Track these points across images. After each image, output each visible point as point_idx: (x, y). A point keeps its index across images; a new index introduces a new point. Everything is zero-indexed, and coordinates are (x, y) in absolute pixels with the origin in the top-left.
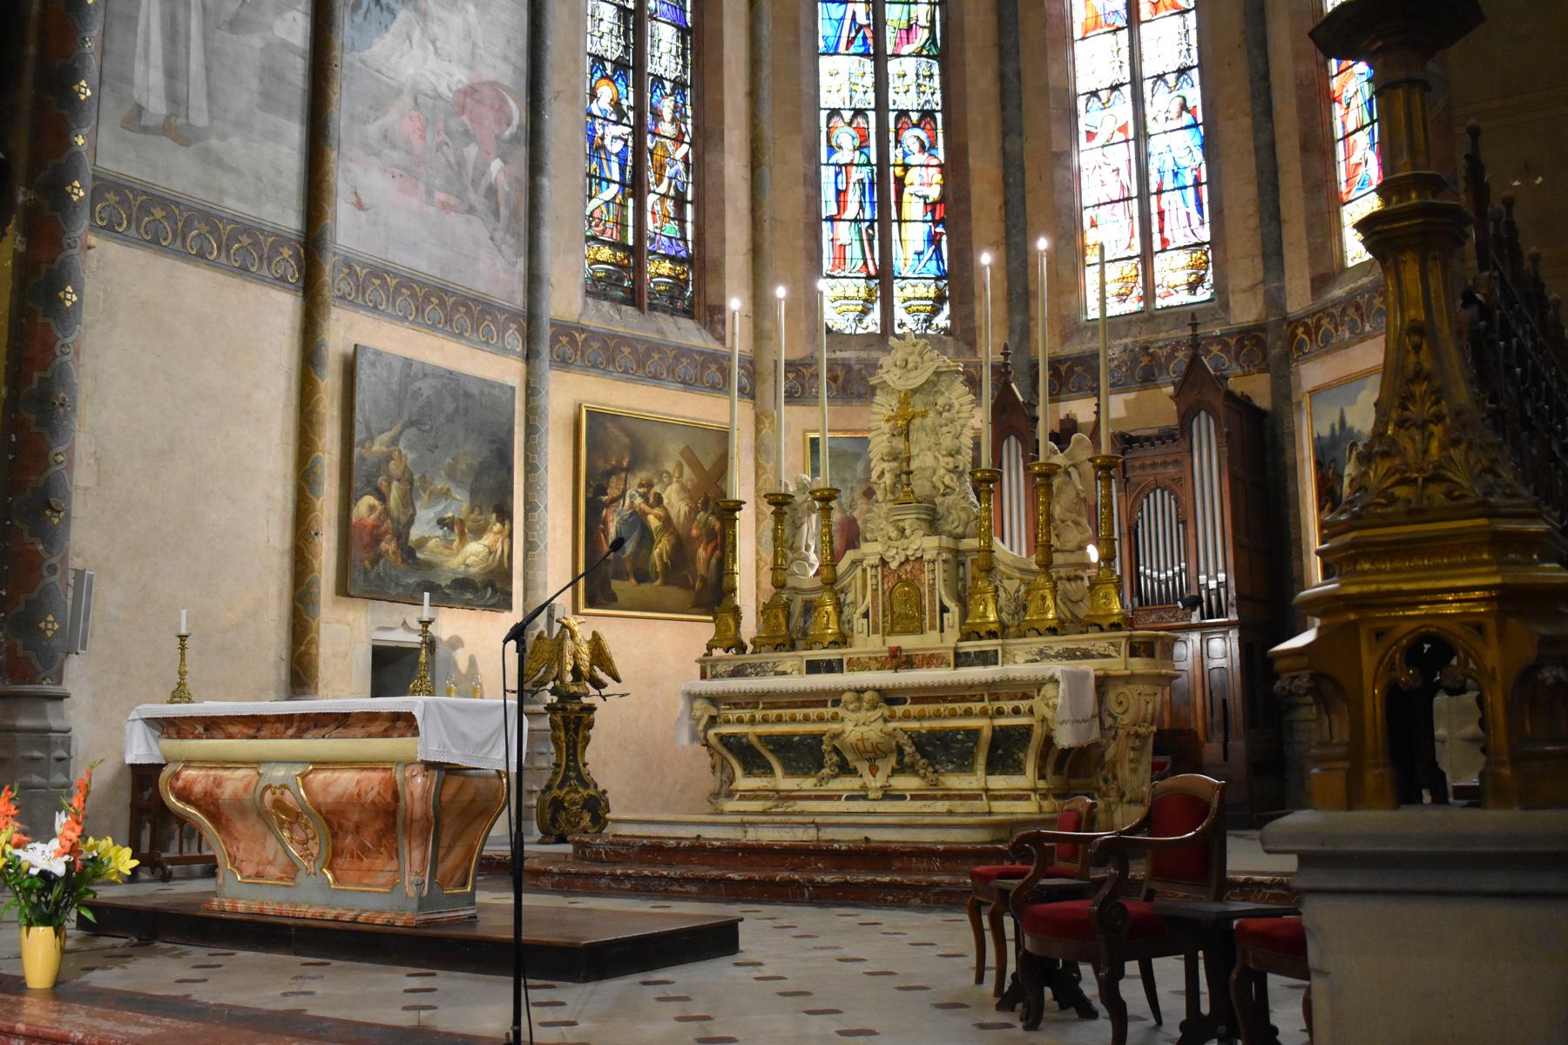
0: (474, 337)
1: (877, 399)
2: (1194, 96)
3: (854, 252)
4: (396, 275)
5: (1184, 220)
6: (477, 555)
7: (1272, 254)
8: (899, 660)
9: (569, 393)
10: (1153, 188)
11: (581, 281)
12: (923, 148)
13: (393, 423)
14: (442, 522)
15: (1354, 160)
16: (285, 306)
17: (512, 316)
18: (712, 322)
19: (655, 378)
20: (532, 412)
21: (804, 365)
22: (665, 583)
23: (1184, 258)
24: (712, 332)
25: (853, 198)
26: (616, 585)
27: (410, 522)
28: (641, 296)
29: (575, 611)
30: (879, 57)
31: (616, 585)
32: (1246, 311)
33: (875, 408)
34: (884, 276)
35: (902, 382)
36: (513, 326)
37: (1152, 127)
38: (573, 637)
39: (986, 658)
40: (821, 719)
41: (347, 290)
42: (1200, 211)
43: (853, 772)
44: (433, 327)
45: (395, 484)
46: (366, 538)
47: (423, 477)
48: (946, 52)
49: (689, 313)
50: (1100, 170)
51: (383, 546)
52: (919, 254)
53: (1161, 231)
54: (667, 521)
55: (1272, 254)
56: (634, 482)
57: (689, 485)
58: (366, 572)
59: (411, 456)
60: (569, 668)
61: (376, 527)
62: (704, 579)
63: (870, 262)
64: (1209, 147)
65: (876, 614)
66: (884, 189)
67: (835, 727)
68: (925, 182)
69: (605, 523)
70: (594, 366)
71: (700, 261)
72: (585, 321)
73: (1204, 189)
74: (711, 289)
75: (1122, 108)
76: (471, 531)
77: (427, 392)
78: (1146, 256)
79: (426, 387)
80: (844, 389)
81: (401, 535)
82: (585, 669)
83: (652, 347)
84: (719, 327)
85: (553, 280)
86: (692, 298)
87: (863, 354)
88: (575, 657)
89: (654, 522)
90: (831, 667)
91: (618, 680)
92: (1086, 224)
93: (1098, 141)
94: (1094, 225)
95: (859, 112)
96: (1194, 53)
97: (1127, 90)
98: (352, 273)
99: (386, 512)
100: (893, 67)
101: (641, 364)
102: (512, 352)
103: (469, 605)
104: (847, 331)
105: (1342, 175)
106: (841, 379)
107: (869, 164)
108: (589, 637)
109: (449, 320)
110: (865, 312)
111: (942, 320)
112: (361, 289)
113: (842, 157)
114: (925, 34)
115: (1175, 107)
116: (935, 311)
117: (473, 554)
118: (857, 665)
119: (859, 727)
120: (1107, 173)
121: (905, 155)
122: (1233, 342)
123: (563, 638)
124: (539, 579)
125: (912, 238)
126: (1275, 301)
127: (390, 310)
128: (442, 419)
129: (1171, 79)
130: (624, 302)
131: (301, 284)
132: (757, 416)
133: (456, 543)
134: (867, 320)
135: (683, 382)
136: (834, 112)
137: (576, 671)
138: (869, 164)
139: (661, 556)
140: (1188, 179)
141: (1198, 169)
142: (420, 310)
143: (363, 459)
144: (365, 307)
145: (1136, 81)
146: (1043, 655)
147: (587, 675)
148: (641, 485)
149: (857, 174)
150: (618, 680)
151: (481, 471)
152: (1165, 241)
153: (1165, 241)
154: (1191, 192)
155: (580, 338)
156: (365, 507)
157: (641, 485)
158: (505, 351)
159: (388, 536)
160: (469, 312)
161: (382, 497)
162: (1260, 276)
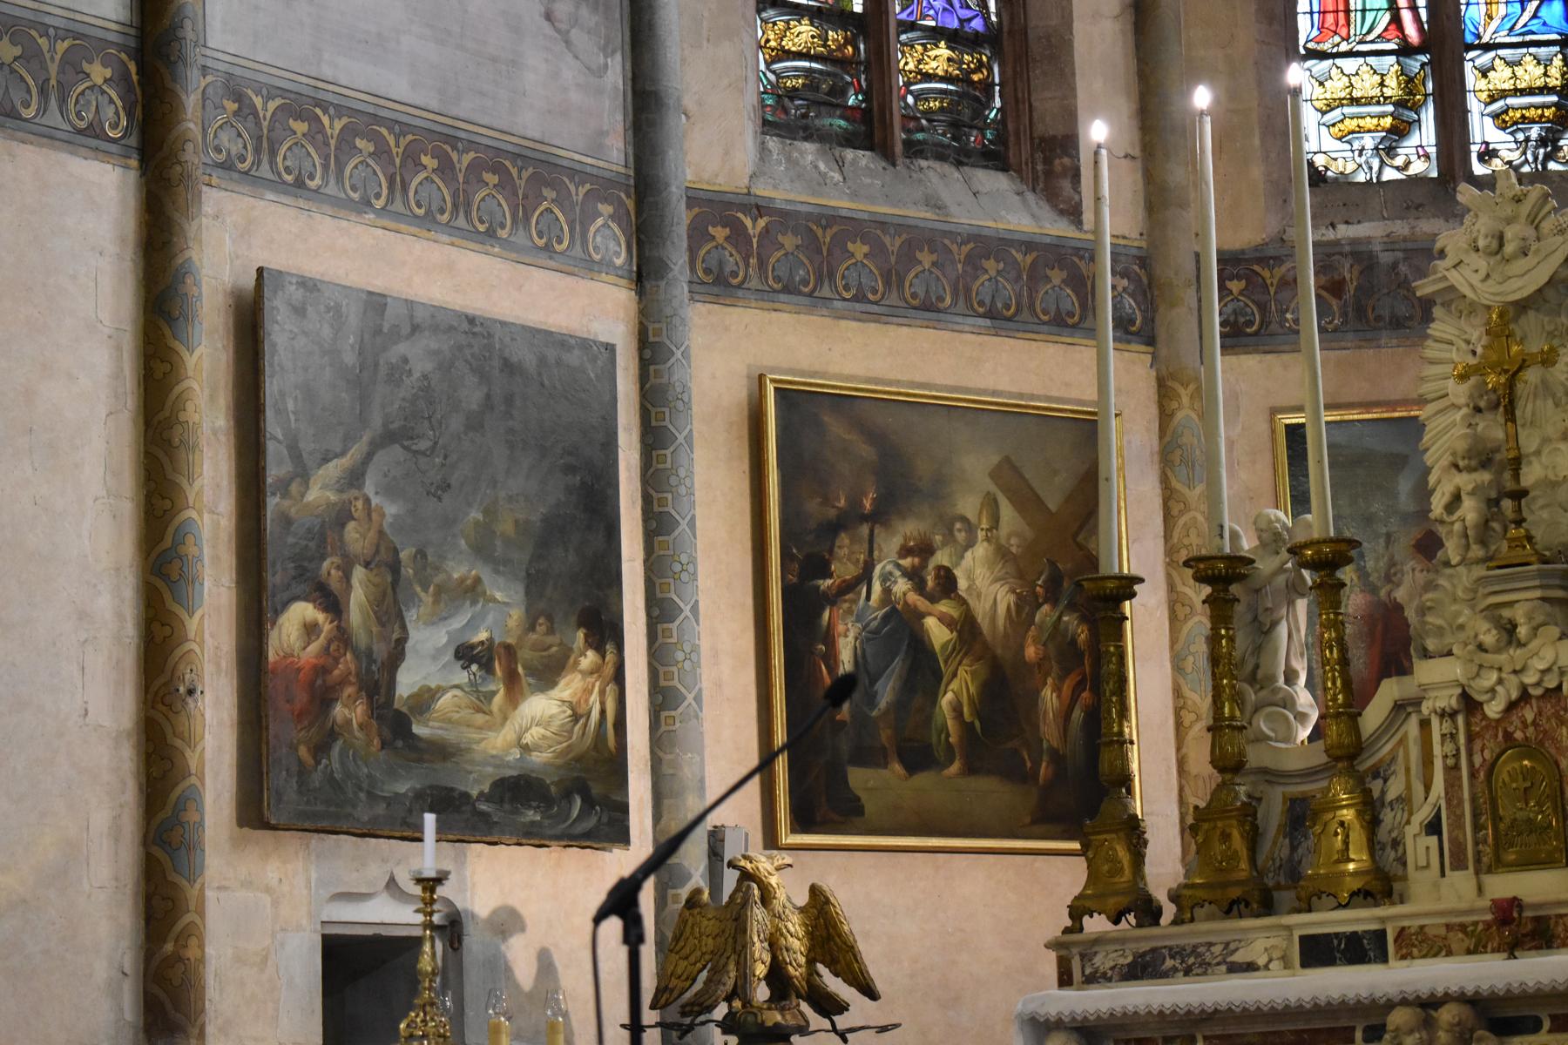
0: (520, 238)
1: (1436, 329)
4: (340, 111)
6: (544, 723)
9: (732, 351)
11: (751, 98)
13: (349, 440)
14: (465, 654)
16: (101, 190)
17: (602, 186)
18: (1049, 174)
19: (928, 309)
20: (656, 400)
21: (1262, 261)
22: (970, 770)
24: (1051, 196)
26: (859, 778)
27: (397, 655)
28: (887, 126)
29: (771, 841)
31: (859, 778)
33: (1432, 350)
35: (1491, 286)
36: (606, 209)
38: (767, 897)
41: (236, 148)
44: (428, 221)
45: (359, 573)
46: (301, 698)
47: (421, 554)
49: (995, 158)
51: (339, 711)
54: (966, 628)
56: (890, 545)
57: (1014, 546)
58: (303, 773)
59: (391, 510)
60: (761, 970)
61: (321, 670)
62: (1056, 757)
63: (1406, 16)
65: (1457, 822)
69: (829, 639)
70: (789, 289)
72: (763, 190)
74: (1044, 102)
76: (532, 671)
77: (421, 366)
79: (419, 355)
80: (1360, 312)
81: (377, 684)
82: (796, 972)
83: (917, 239)
84: (1066, 184)
85: (689, 102)
86: (1001, 123)
87: (1401, 228)
88: (773, 944)
89: (938, 633)
90: (1359, 949)
91: (870, 992)
98: (246, 111)
99: (343, 636)
101: (893, 278)
102: (605, 266)
103: (534, 836)
104: (1361, 177)
106: (1351, 288)
108: (802, 899)
109: (462, 204)
110: (1400, 130)
112: (266, 145)
117: (538, 721)
118: (1417, 943)
123: (745, 903)
124: (687, 772)
127: (331, 189)
128: (456, 423)
130: (849, 141)
131: (133, 141)
132: (1161, 383)
133: (498, 699)
134: (1408, 148)
135: (991, 314)
137: (777, 976)
139: (957, 709)
142: (398, 185)
143: (286, 521)
144: (278, 186)
147: (801, 984)
148: (905, 551)
150: (870, 992)
151: (549, 534)
155: (754, 227)
156: (295, 627)
157: (905, 551)
158: (590, 267)
159: (349, 690)
160: (506, 184)
161: (333, 604)
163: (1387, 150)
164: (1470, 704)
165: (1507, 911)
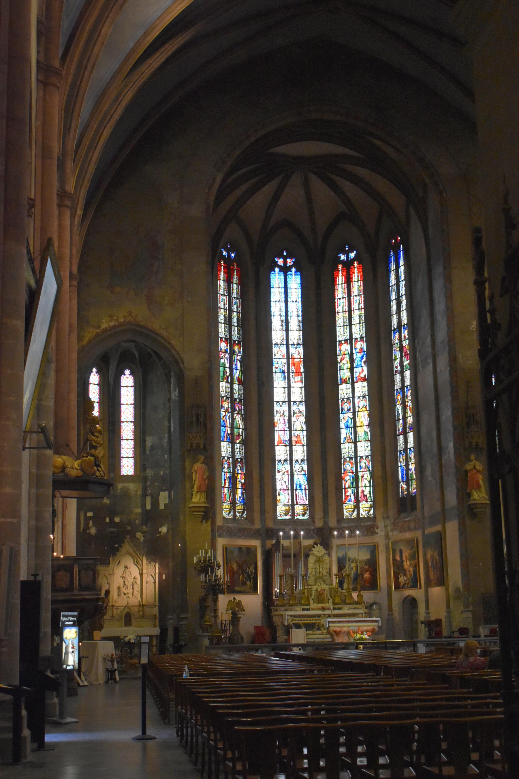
2: (305, 468)
3: (227, 496)
5: (302, 497)
7: (326, 512)
8: (323, 609)
10: (295, 488)
12: (241, 469)
15: (348, 494)
23: (301, 508)
25: (227, 481)
32: (319, 524)
37: (295, 473)
39: (339, 609)
40: (316, 620)
42: (306, 496)
43: (320, 630)
50: (282, 481)
52: (240, 497)
53: (296, 500)
55: (326, 512)
64: (310, 480)
66: (233, 479)
67: (319, 621)
68: (241, 479)
73: (307, 491)
75: (287, 467)
78: (293, 505)
90: (307, 610)
92: (277, 494)
93: (281, 473)
94: (279, 495)
95: (229, 458)
96: (306, 456)
97: (288, 462)
105: (344, 497)
107: (230, 472)
110: (230, 512)
111: (244, 515)
113: (225, 470)
114: (241, 438)
115: (300, 470)
116: (243, 513)
120: (283, 481)
121: (238, 470)
122: (316, 531)
126: (326, 523)
129: (300, 461)
136: (224, 457)
138: (230, 472)
140: (303, 488)
141: (306, 486)
146: (350, 608)
152: (297, 503)
153: (297, 503)
154: (304, 491)
162: (322, 516)
163: (229, 515)
164: (317, 590)
165: (323, 607)
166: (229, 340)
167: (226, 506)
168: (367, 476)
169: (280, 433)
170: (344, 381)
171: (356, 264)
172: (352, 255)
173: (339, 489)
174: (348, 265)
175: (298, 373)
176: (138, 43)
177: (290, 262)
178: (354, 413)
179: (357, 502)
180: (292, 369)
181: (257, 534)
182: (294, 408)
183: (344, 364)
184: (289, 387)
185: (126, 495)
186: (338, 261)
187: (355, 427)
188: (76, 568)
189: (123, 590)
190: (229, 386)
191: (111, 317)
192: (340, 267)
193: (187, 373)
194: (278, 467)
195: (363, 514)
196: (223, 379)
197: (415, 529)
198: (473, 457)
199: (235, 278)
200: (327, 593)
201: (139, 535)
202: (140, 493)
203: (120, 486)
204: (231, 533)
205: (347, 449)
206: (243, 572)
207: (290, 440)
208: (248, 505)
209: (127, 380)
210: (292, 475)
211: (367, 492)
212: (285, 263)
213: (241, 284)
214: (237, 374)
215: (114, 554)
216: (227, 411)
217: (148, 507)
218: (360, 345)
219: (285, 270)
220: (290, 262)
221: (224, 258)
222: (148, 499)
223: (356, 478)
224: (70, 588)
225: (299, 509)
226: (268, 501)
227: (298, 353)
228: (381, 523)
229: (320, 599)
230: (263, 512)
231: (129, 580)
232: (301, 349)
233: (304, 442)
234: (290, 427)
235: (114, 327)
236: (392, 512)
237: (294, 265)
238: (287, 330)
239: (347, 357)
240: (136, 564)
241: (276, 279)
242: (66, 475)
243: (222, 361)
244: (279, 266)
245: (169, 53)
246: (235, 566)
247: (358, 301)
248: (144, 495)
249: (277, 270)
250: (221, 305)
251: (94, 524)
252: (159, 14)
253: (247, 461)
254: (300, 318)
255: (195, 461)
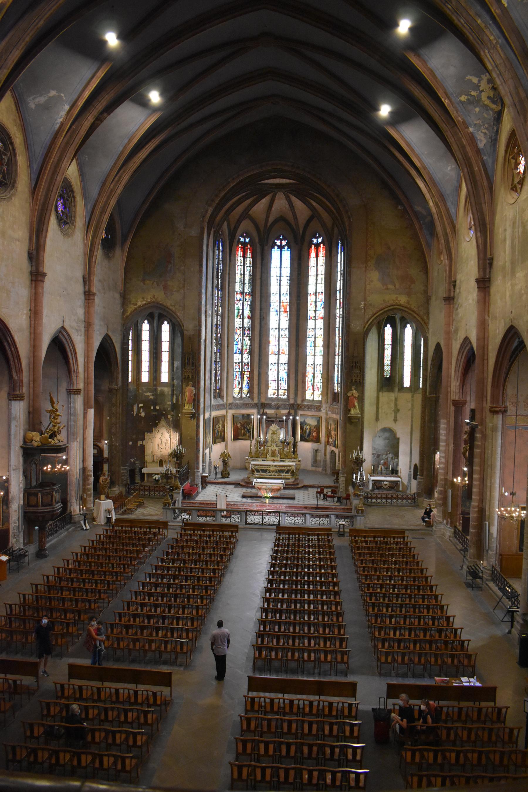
2: (287, 368)
5: (284, 386)
7: (296, 395)
8: (274, 461)
30: (242, 354)
32: (292, 401)
34: (241, 389)
48: (251, 353)
50: (272, 375)
55: (296, 395)
64: (288, 376)
66: (242, 375)
68: (247, 374)
71: (221, 389)
75: (276, 367)
78: (278, 390)
100: (244, 356)
119: (272, 469)
125: (245, 382)
126: (296, 401)
145: (278, 363)
149: (239, 373)
166: (242, 293)
167: (236, 390)
168: (320, 376)
169: (272, 348)
170: (311, 318)
171: (322, 246)
172: (320, 240)
173: (304, 382)
174: (317, 246)
175: (285, 311)
176: (125, 147)
177: (284, 243)
178: (315, 338)
179: (314, 390)
180: (282, 309)
181: (255, 406)
182: (282, 332)
183: (311, 308)
184: (279, 320)
185: (162, 394)
186: (311, 243)
187: (315, 346)
188: (40, 495)
189: (160, 446)
190: (241, 320)
191: (143, 298)
192: (313, 246)
193: (185, 332)
194: (271, 367)
195: (316, 398)
196: (238, 316)
197: (337, 414)
198: (353, 388)
199: (248, 255)
200: (277, 452)
201: (169, 416)
202: (170, 393)
203: (159, 389)
204: (237, 407)
205: (310, 360)
206: (244, 428)
207: (279, 352)
208: (251, 390)
209: (166, 327)
210: (278, 372)
211: (319, 386)
212: (281, 243)
213: (253, 257)
214: (247, 313)
215: (156, 427)
216: (239, 335)
217: (175, 402)
218: (321, 297)
219: (281, 248)
220: (284, 243)
221: (241, 243)
222: (175, 397)
223: (314, 377)
224: (36, 506)
225: (281, 392)
226: (263, 387)
227: (286, 299)
228: (324, 405)
229: (273, 454)
230: (259, 393)
231: (164, 441)
232: (288, 297)
233: (287, 353)
234: (279, 344)
235: (145, 304)
236: (330, 400)
237: (287, 244)
238: (280, 285)
239: (313, 304)
240: (168, 432)
241: (275, 253)
242: (32, 445)
243: (236, 306)
244: (278, 246)
245: (152, 148)
246: (239, 425)
247: (322, 269)
248: (173, 395)
249: (276, 247)
250: (238, 272)
251: (143, 411)
252: (137, 127)
253: (251, 364)
254: (289, 278)
255: (188, 385)
